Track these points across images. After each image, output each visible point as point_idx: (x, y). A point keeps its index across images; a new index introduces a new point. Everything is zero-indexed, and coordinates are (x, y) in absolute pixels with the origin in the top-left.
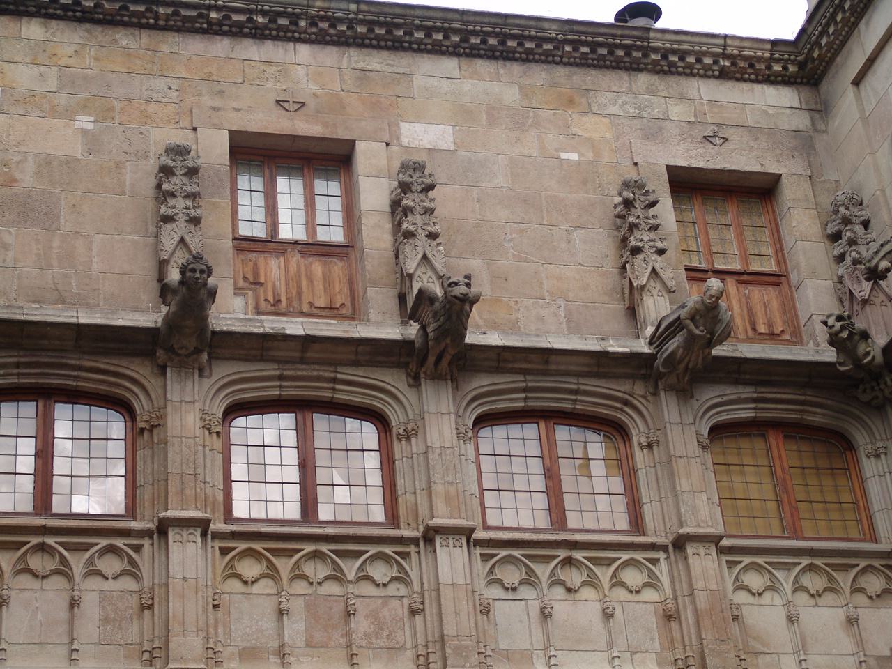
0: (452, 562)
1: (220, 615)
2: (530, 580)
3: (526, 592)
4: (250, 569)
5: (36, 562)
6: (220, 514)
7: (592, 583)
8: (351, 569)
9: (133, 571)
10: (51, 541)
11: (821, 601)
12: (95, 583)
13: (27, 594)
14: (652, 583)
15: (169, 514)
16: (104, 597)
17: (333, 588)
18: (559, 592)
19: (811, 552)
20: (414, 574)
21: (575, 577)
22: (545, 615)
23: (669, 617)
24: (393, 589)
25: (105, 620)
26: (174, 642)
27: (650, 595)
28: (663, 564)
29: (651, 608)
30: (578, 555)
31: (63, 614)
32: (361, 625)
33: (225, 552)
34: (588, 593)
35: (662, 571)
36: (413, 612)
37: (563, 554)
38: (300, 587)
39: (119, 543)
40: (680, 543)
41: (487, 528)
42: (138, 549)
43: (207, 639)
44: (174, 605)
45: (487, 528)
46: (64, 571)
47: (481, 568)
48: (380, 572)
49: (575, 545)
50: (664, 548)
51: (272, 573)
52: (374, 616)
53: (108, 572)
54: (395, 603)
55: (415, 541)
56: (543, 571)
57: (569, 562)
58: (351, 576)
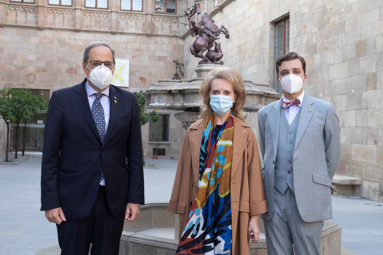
0: (114, 16)
1: (83, 21)
2: (125, 18)
3: (125, 20)
4: (87, 14)
5: (59, 12)
6: (84, 7)
7: (134, 19)
8: (101, 15)
9: (72, 14)
10: (61, 10)
11: (166, 23)
12: (67, 16)
13: (58, 17)
14: (142, 19)
15: (76, 8)
16: (68, 18)
17: (98, 18)
18: (129, 20)
19: (166, 16)
20: (109, 17)
21: (132, 18)
22: (127, 23)
23: (144, 24)
24: (107, 18)
25: (68, 21)
26: (76, 25)
27: (142, 21)
28: (144, 17)
29: (142, 23)
30: (133, 15)
31: (63, 20)
32: (102, 23)
33: (84, 12)
34: (133, 20)
35: (144, 18)
36: (109, 22)
37: (130, 14)
38: (94, 17)
39: (70, 10)
40: (147, 14)
41: (121, 10)
42: (72, 11)
43: (81, 25)
44: (76, 20)
45: (121, 10)
46: (63, 14)
47: (119, 16)
48: (105, 16)
49: (132, 13)
50: (145, 14)
51: (90, 15)
52: (104, 22)
53: (68, 14)
54: (107, 20)
55: (110, 12)
56: (127, 17)
57: (131, 16)
58: (101, 16)
